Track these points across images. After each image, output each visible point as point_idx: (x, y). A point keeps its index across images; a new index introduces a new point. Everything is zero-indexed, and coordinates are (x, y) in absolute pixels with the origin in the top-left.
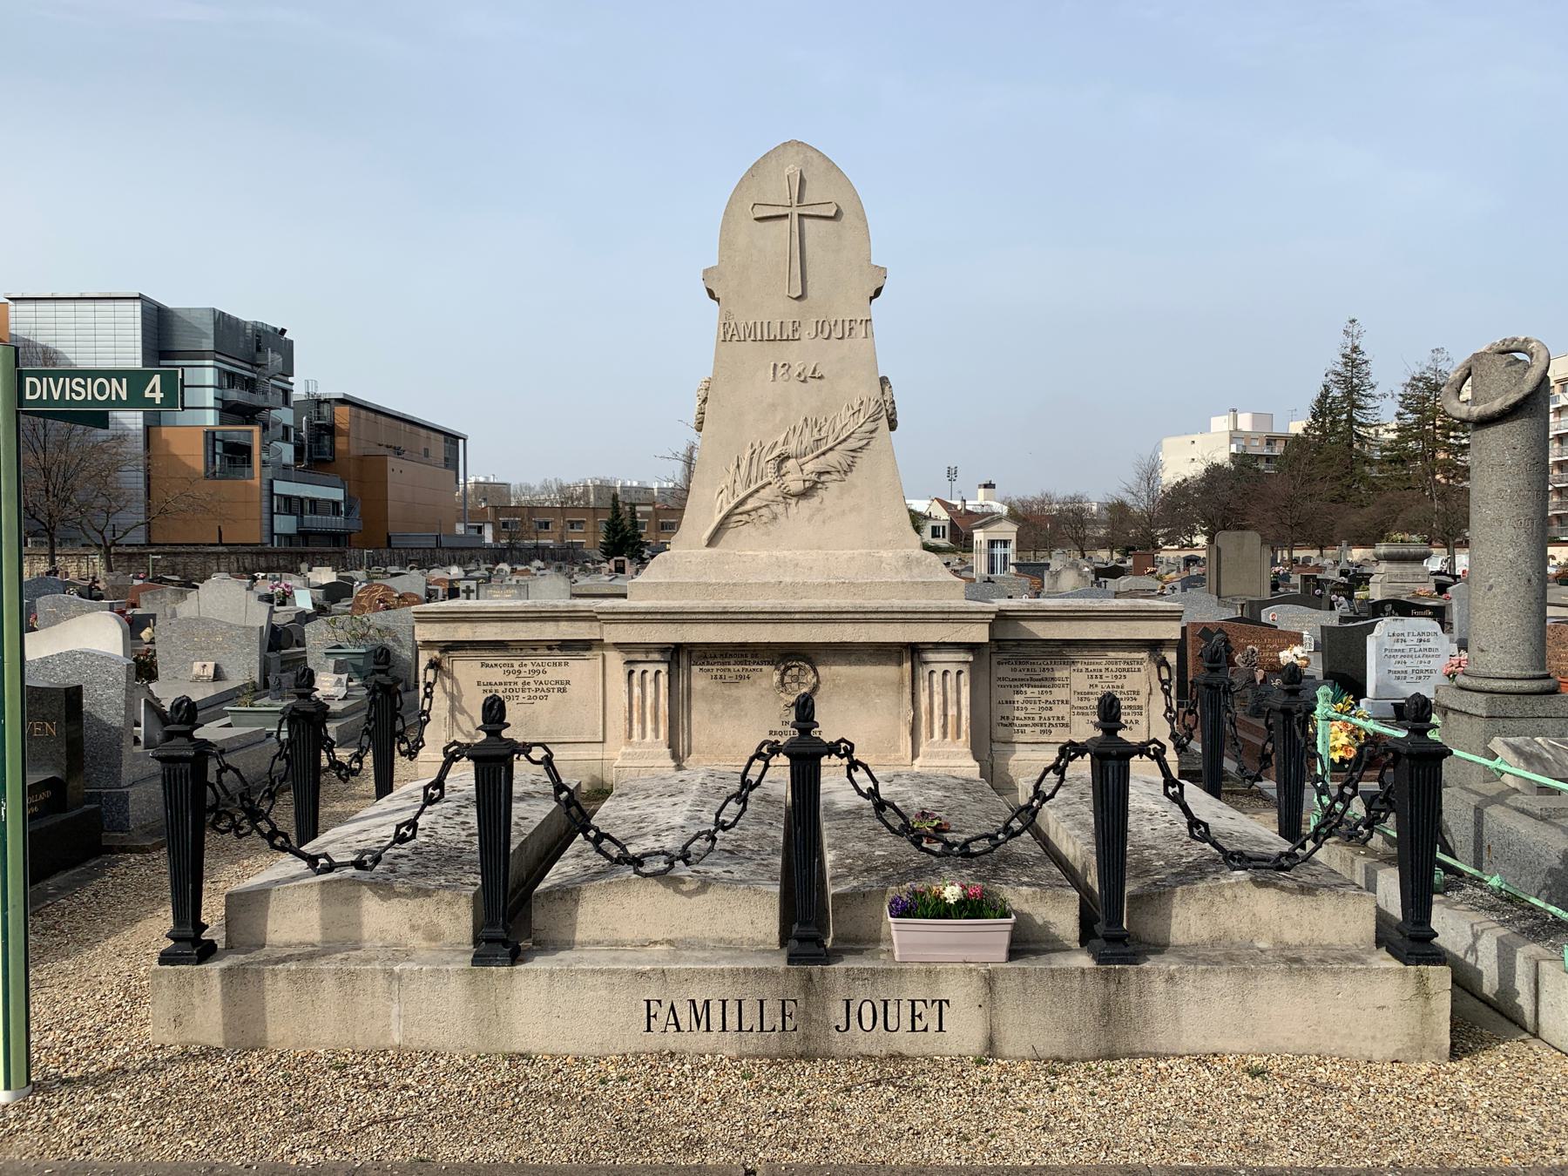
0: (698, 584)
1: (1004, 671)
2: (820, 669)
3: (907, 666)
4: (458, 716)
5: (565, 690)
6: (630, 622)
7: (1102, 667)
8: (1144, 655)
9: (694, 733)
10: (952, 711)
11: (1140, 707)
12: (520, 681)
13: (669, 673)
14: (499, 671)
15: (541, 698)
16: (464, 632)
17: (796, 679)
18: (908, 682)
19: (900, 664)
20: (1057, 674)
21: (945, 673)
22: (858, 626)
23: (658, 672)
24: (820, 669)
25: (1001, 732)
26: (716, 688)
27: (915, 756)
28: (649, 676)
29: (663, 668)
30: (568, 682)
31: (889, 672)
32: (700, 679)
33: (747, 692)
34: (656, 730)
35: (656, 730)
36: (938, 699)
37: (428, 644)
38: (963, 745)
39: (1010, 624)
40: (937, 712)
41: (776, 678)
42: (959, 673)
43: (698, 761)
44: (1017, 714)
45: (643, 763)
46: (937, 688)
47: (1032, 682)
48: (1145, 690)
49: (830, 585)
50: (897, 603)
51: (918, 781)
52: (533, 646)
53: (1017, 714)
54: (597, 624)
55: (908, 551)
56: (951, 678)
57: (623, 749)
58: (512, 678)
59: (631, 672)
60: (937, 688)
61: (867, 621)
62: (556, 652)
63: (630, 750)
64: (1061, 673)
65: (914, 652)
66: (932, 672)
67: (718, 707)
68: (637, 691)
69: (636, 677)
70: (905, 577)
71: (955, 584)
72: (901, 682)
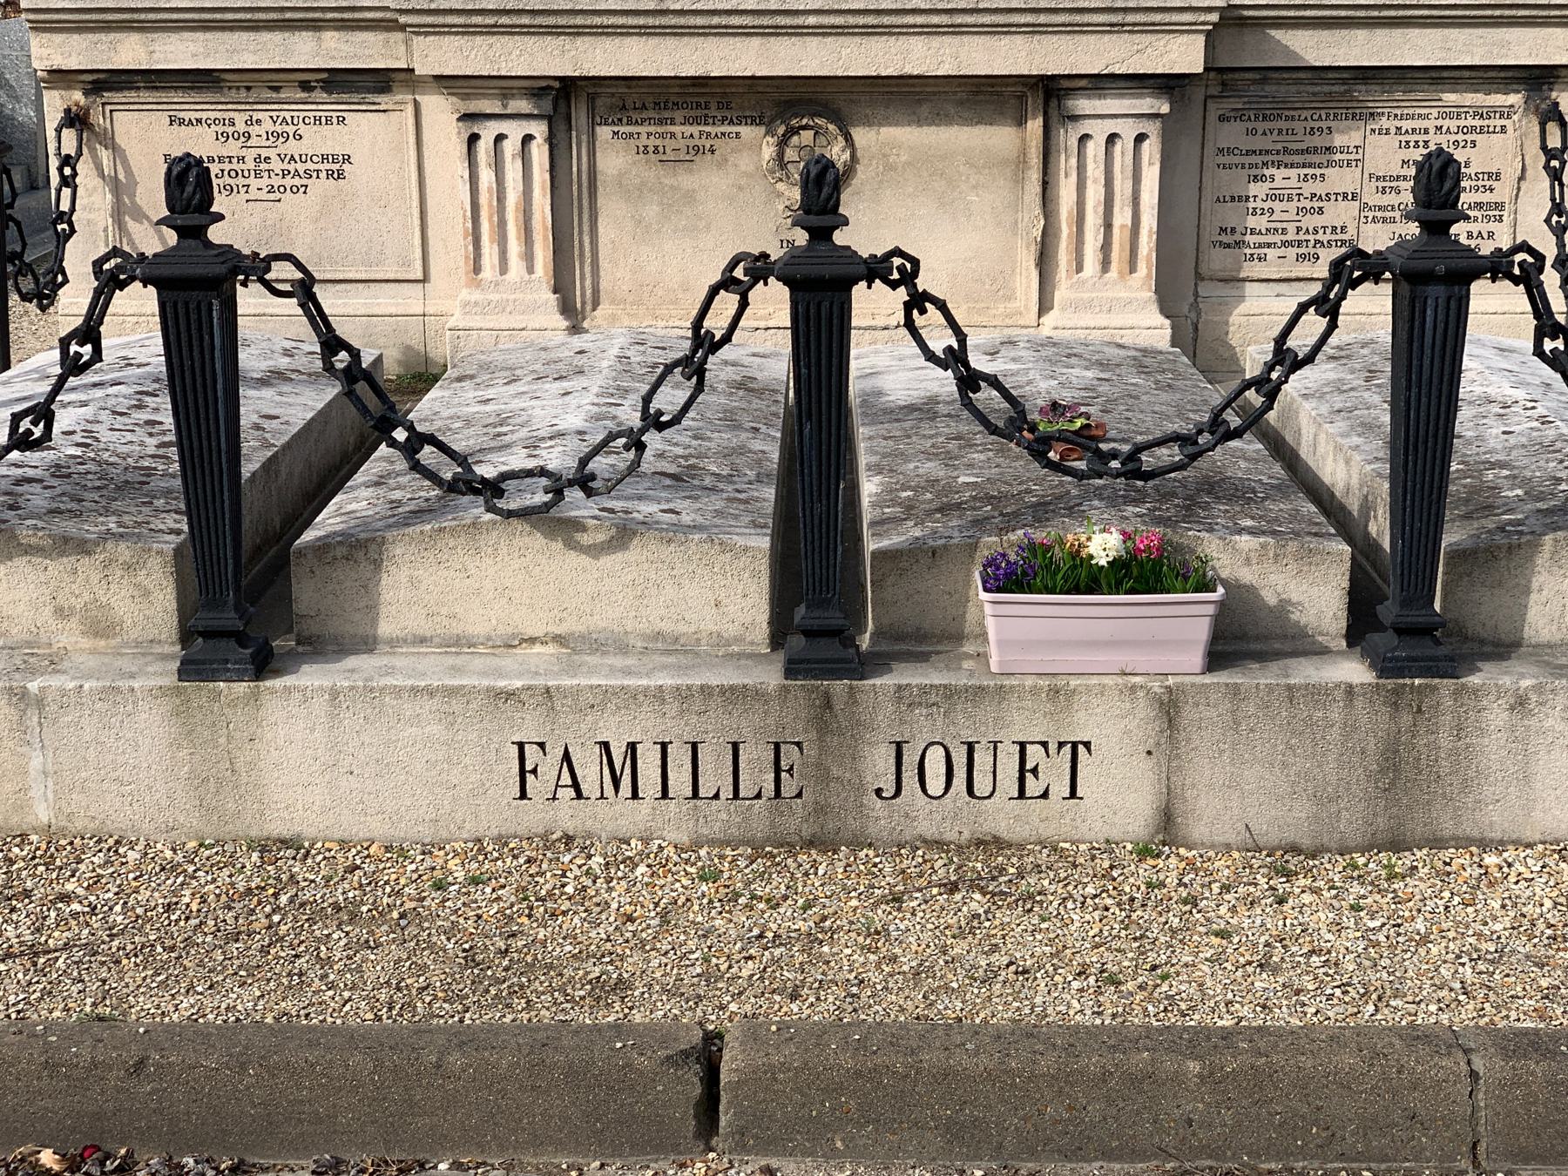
1: (1232, 134)
2: (860, 135)
3: (1035, 126)
4: (131, 225)
5: (340, 175)
6: (467, 31)
7: (1430, 124)
8: (1515, 99)
9: (604, 263)
10: (1122, 218)
11: (1499, 206)
12: (250, 155)
13: (551, 140)
14: (208, 133)
15: (295, 190)
16: (130, 52)
18: (1035, 159)
19: (1021, 122)
20: (1339, 140)
21: (1112, 138)
22: (936, 41)
23: (528, 139)
24: (860, 135)
25: (1217, 260)
26: (649, 172)
27: (1044, 307)
28: (511, 147)
29: (539, 129)
30: (347, 159)
31: (998, 138)
32: (614, 154)
34: (529, 257)
35: (529, 257)
36: (1095, 194)
37: (60, 77)
38: (1141, 285)
39: (1250, 37)
40: (1093, 220)
41: (768, 151)
42: (1140, 138)
44: (1252, 222)
45: (504, 321)
46: (1095, 171)
47: (1284, 157)
48: (1511, 172)
51: (1050, 351)
52: (271, 82)
53: (1252, 222)
54: (399, 36)
57: (465, 294)
58: (233, 148)
59: (473, 139)
60: (1095, 171)
61: (956, 30)
62: (320, 95)
63: (476, 296)
64: (1346, 137)
65: (1050, 95)
66: (1084, 138)
67: (651, 211)
68: (486, 176)
69: (484, 146)
72: (1022, 161)
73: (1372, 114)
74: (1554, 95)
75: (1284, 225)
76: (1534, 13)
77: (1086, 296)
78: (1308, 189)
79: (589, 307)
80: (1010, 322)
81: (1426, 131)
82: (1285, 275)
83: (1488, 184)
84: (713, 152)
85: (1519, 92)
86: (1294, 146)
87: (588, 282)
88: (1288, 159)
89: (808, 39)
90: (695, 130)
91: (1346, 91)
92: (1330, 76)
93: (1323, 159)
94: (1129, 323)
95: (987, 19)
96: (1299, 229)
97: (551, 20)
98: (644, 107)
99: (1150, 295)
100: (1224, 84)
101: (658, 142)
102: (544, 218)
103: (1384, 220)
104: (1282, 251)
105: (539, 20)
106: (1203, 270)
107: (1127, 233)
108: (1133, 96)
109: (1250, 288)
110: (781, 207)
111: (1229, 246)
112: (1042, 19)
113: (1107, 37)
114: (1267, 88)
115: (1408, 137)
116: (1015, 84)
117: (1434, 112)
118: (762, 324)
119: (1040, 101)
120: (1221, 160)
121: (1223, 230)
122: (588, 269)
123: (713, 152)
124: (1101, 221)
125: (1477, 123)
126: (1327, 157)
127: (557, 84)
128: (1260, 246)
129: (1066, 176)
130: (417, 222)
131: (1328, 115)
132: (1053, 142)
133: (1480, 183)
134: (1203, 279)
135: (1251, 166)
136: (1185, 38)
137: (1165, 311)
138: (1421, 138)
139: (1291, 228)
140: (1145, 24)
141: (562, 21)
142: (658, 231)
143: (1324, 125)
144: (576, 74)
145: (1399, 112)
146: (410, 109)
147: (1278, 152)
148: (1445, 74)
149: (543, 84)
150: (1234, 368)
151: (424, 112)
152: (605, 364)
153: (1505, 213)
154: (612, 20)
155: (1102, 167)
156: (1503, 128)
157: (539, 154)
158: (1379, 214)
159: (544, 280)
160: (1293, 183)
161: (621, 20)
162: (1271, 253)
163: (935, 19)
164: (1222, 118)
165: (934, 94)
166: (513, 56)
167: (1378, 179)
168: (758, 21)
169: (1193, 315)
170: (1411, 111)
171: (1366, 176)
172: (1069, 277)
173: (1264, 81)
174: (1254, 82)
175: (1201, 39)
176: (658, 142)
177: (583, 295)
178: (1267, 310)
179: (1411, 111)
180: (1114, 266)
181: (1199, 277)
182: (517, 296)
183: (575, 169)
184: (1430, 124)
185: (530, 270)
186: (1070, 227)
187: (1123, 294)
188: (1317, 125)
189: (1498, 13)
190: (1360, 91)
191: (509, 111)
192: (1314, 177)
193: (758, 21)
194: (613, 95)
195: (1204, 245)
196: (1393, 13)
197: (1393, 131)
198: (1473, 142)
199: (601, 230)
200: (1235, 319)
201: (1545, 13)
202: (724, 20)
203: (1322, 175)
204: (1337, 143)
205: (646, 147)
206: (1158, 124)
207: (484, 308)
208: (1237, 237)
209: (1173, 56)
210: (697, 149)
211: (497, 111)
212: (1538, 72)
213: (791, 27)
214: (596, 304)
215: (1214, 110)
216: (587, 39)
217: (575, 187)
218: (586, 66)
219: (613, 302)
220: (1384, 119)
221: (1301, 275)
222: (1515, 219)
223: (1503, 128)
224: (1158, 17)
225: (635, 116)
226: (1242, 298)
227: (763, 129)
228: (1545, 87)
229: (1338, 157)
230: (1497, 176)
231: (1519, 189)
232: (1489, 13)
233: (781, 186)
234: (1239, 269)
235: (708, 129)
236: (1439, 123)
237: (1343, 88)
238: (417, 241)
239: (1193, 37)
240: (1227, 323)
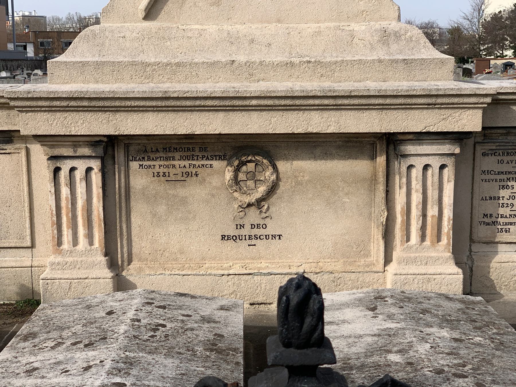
0: (133, 64)
1: (490, 163)
2: (281, 165)
3: (381, 160)
6: (51, 110)
9: (134, 238)
10: (432, 211)
13: (103, 171)
17: (252, 176)
18: (382, 179)
19: (373, 157)
21: (426, 167)
22: (326, 114)
23: (89, 170)
24: (281, 165)
25: (482, 232)
27: (388, 260)
29: (96, 165)
31: (360, 166)
32: (140, 177)
33: (195, 192)
34: (90, 237)
35: (90, 237)
36: (416, 198)
38: (444, 249)
40: (415, 212)
41: (229, 175)
42: (443, 167)
43: (140, 270)
44: (501, 211)
45: (75, 274)
46: (416, 185)
49: (292, 64)
50: (373, 85)
51: (409, 308)
53: (501, 211)
54: (15, 112)
55: (384, 24)
56: (432, 175)
57: (52, 258)
59: (57, 170)
60: (416, 185)
61: (338, 108)
63: (59, 259)
65: (391, 143)
66: (410, 167)
67: (162, 209)
68: (65, 191)
69: (64, 174)
70: (381, 54)
71: (442, 62)
72: (374, 179)
77: (412, 255)
79: (126, 264)
80: (368, 269)
84: (197, 175)
87: (125, 249)
89: (252, 113)
90: (186, 163)
94: (439, 271)
95: (356, 101)
97: (101, 103)
98: (157, 151)
99: (449, 254)
100: (485, 135)
101: (165, 170)
102: (99, 214)
105: (93, 103)
106: (475, 237)
107: (436, 220)
108: (438, 144)
110: (236, 206)
112: (388, 101)
113: (425, 111)
114: (509, 138)
116: (370, 137)
118: (226, 272)
119: (384, 146)
120: (484, 177)
121: (485, 215)
122: (125, 242)
123: (197, 175)
124: (420, 213)
127: (105, 139)
128: (506, 224)
129: (400, 188)
130: (27, 214)
132: (391, 169)
134: (474, 242)
135: (501, 180)
136: (471, 112)
137: (458, 264)
140: (448, 104)
141: (107, 103)
142: (166, 220)
144: (116, 134)
146: (23, 153)
149: (98, 139)
150: (493, 292)
151: (32, 153)
152: (123, 328)
154: (137, 103)
155: (421, 183)
157: (96, 178)
159: (99, 249)
161: (142, 103)
163: (326, 102)
164: (484, 154)
165: (324, 142)
166: (79, 124)
168: (222, 103)
169: (469, 262)
172: (402, 244)
173: (507, 134)
174: (502, 134)
175: (480, 113)
176: (165, 170)
177: (122, 257)
178: (511, 260)
180: (428, 238)
181: (472, 241)
182: (84, 258)
183: (117, 186)
185: (91, 243)
186: (402, 216)
187: (433, 254)
191: (78, 154)
193: (222, 103)
194: (139, 144)
195: (475, 223)
199: (133, 219)
200: (493, 264)
202: (203, 103)
205: (158, 173)
206: (453, 159)
207: (63, 266)
208: (493, 219)
209: (464, 122)
210: (188, 174)
211: (71, 154)
213: (242, 106)
214: (130, 262)
215: (480, 149)
216: (122, 114)
217: (117, 196)
218: (122, 129)
219: (140, 260)
224: (456, 100)
225: (152, 156)
226: (496, 253)
227: (225, 163)
233: (236, 194)
235: (194, 162)
238: (28, 225)
239: (476, 111)
240: (489, 267)
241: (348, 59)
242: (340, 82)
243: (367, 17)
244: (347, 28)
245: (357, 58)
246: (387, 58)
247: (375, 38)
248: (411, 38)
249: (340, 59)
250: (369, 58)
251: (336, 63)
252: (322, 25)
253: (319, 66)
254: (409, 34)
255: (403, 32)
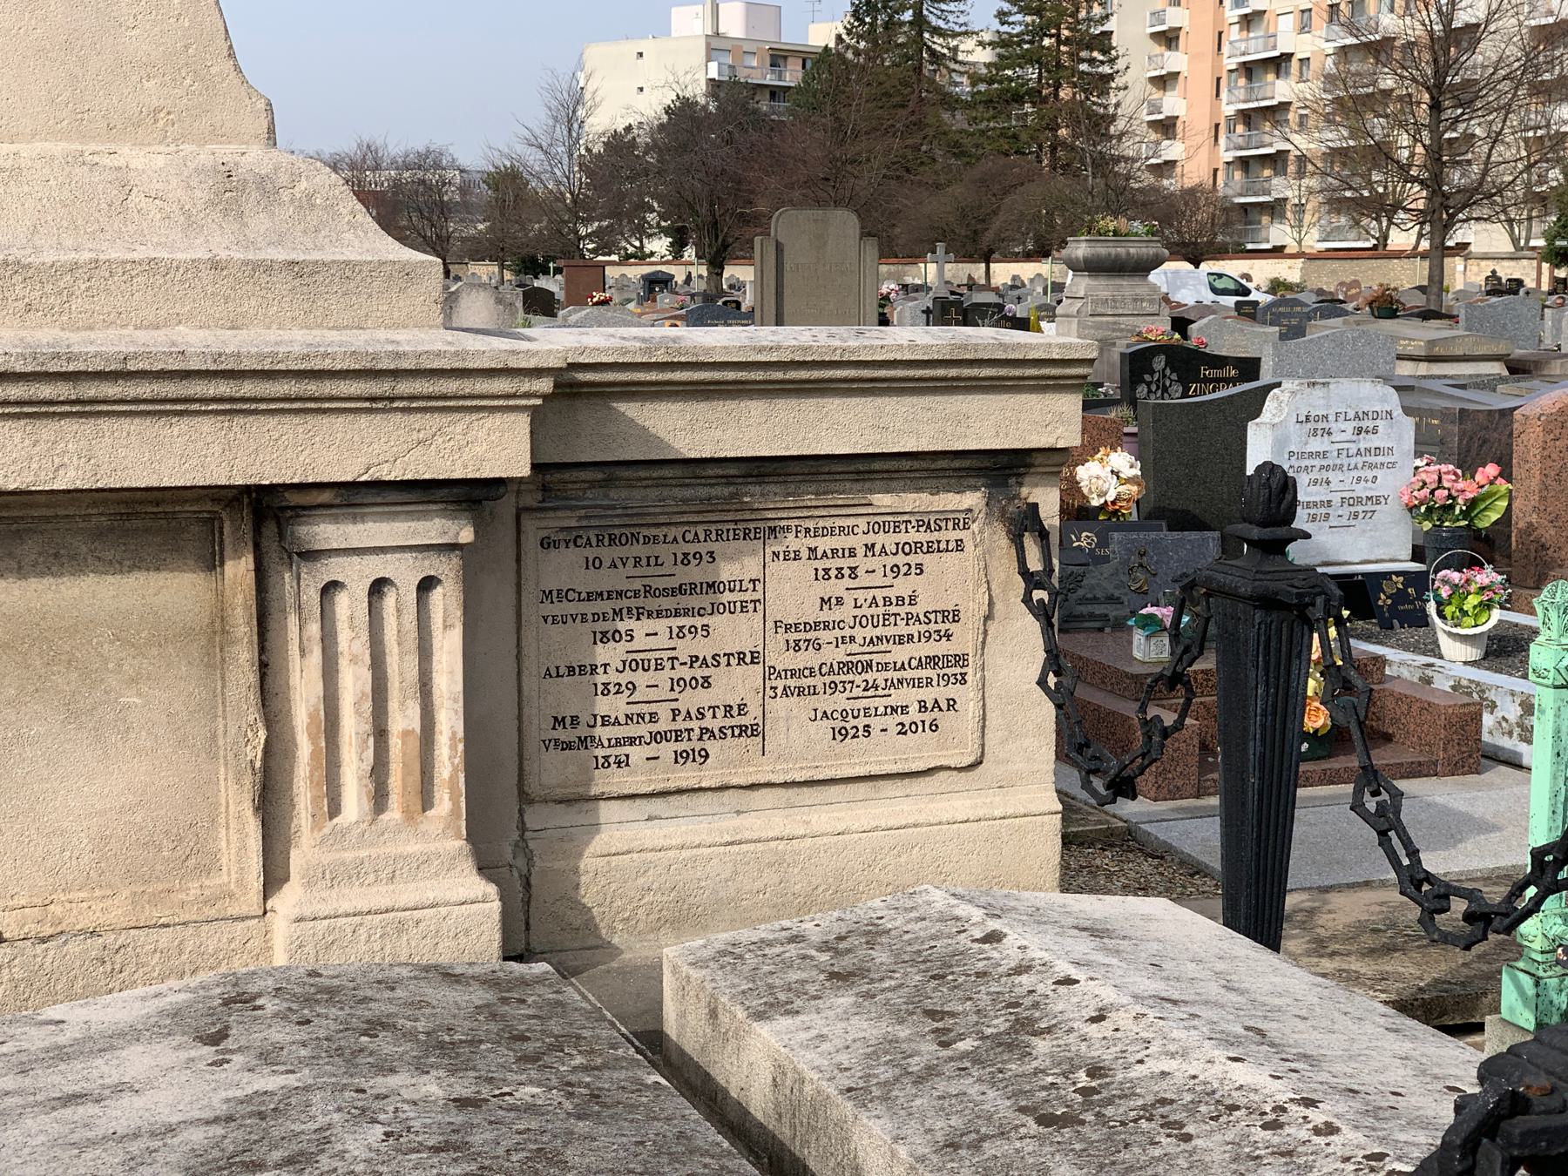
1: (563, 568)
3: (239, 569)
7: (857, 541)
8: (972, 499)
10: (403, 718)
11: (961, 660)
19: (212, 562)
20: (727, 571)
21: (378, 587)
22: (47, 430)
25: (552, 769)
31: (172, 592)
36: (354, 681)
38: (442, 828)
39: (586, 414)
40: (353, 725)
42: (426, 585)
44: (603, 706)
46: (352, 642)
47: (648, 600)
48: (973, 609)
50: (197, 340)
51: (328, 1020)
53: (603, 706)
55: (226, 152)
56: (398, 608)
60: (352, 642)
61: (86, 410)
64: (738, 565)
65: (266, 518)
70: (220, 243)
71: (407, 273)
72: (219, 627)
73: (773, 530)
74: (1024, 491)
75: (653, 708)
76: (1003, 372)
77: (349, 856)
78: (685, 648)
80: (212, 912)
81: (852, 553)
82: (660, 787)
83: (942, 627)
85: (976, 488)
86: (661, 583)
88: (652, 604)
91: (733, 496)
92: (710, 472)
93: (703, 601)
94: (431, 896)
95: (145, 389)
96: (675, 713)
99: (457, 844)
100: (545, 488)
103: (801, 691)
104: (651, 750)
106: (533, 787)
107: (414, 745)
108: (410, 516)
109: (607, 811)
111: (568, 746)
112: (248, 388)
113: (364, 420)
114: (613, 493)
115: (827, 563)
116: (197, 500)
117: (862, 523)
119: (247, 527)
120: (549, 609)
121: (559, 721)
124: (368, 727)
125: (923, 537)
126: (711, 597)
128: (619, 743)
129: (303, 652)
131: (707, 534)
132: (273, 594)
133: (932, 627)
134: (531, 802)
135: (596, 617)
136: (497, 420)
137: (485, 868)
138: (845, 563)
139: (664, 711)
140: (430, 398)
143: (703, 548)
145: (811, 524)
147: (636, 594)
148: (877, 466)
150: (591, 942)
153: (969, 670)
155: (365, 636)
156: (959, 542)
158: (792, 683)
160: (663, 641)
162: (636, 753)
163: (46, 391)
164: (546, 544)
165: (47, 519)
167: (788, 628)
169: (521, 862)
170: (828, 523)
171: (770, 624)
172: (317, 826)
173: (608, 483)
174: (593, 484)
175: (522, 423)
178: (636, 845)
179: (828, 523)
180: (395, 800)
181: (525, 798)
184: (857, 541)
186: (313, 739)
187: (413, 848)
188: (691, 548)
189: (953, 372)
190: (753, 495)
192: (693, 630)
195: (532, 745)
196: (804, 374)
197: (805, 554)
198: (919, 566)
200: (588, 863)
201: (1017, 372)
203: (705, 627)
204: (725, 577)
206: (455, 560)
208: (582, 731)
209: (479, 449)
212: (1005, 459)
215: (533, 530)
220: (791, 536)
221: (684, 784)
222: (983, 678)
223: (959, 542)
224: (451, 386)
226: (595, 827)
228: (1012, 481)
229: (727, 597)
230: (954, 616)
231: (985, 632)
232: (941, 372)
234: (589, 781)
236: (871, 538)
237: (726, 491)
239: (512, 417)
240: (576, 871)
241: (114, 255)
242: (91, 328)
243: (170, 129)
244: (107, 161)
245: (141, 253)
246: (238, 255)
247: (198, 193)
248: (310, 197)
249: (86, 256)
250: (180, 256)
251: (74, 267)
252: (27, 150)
253: (18, 278)
254: (304, 185)
255: (284, 179)
